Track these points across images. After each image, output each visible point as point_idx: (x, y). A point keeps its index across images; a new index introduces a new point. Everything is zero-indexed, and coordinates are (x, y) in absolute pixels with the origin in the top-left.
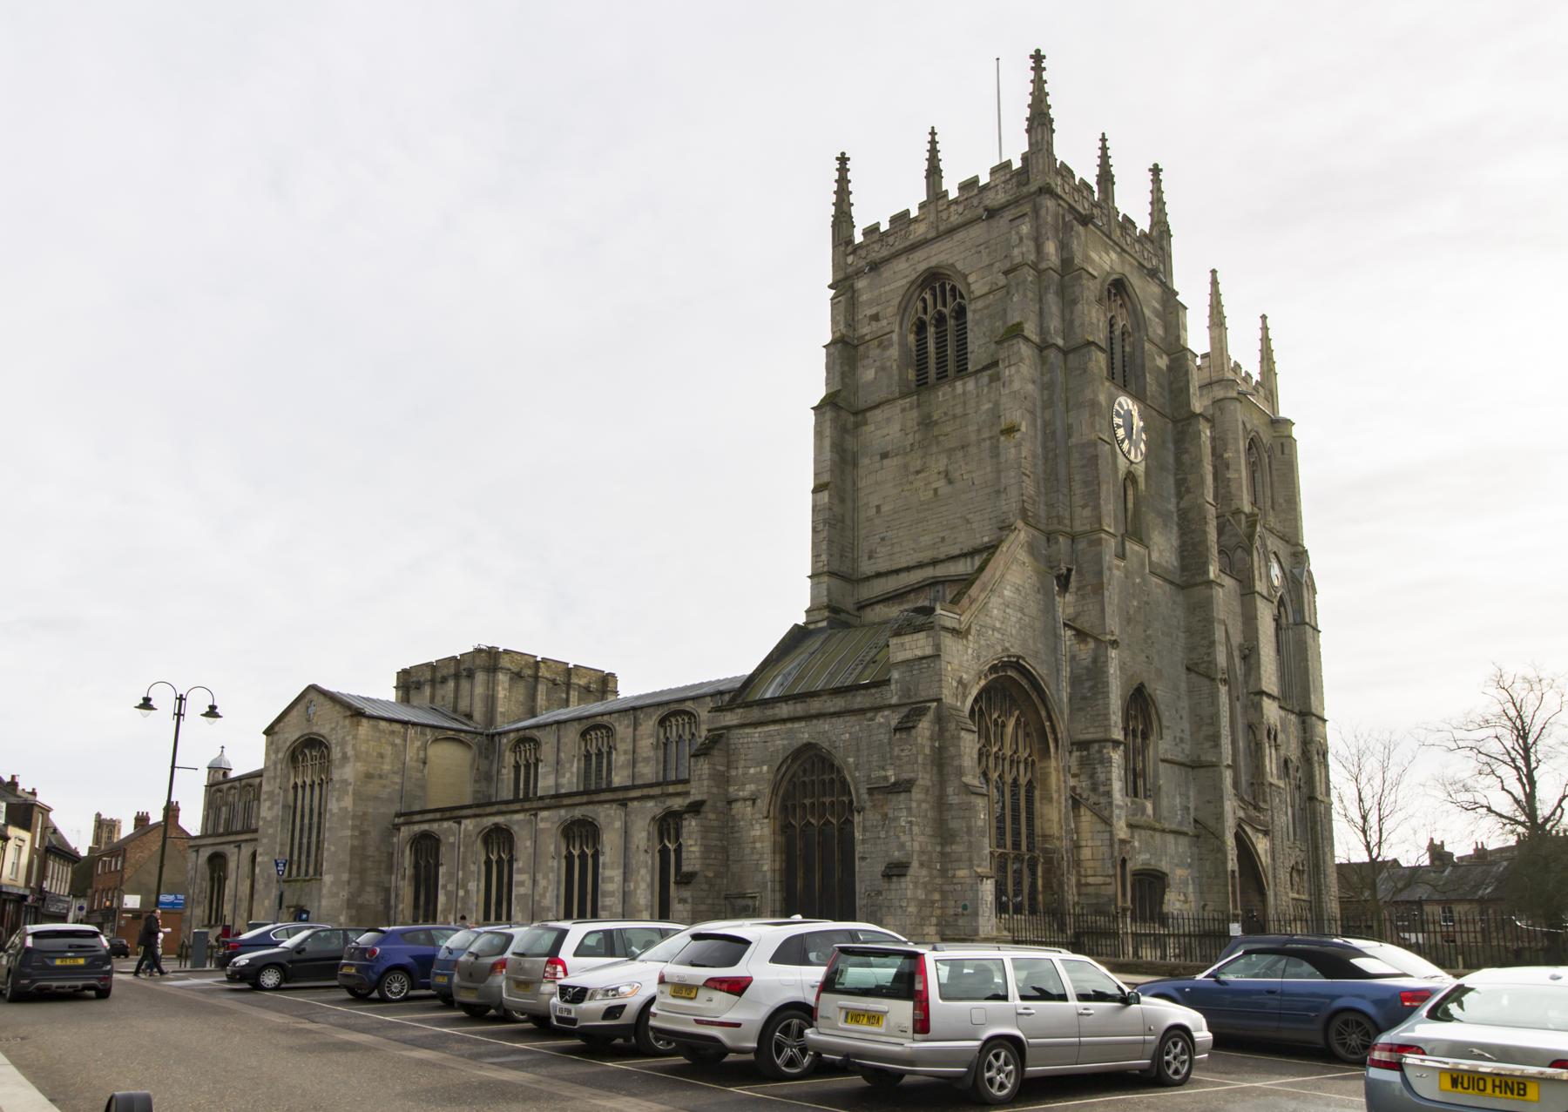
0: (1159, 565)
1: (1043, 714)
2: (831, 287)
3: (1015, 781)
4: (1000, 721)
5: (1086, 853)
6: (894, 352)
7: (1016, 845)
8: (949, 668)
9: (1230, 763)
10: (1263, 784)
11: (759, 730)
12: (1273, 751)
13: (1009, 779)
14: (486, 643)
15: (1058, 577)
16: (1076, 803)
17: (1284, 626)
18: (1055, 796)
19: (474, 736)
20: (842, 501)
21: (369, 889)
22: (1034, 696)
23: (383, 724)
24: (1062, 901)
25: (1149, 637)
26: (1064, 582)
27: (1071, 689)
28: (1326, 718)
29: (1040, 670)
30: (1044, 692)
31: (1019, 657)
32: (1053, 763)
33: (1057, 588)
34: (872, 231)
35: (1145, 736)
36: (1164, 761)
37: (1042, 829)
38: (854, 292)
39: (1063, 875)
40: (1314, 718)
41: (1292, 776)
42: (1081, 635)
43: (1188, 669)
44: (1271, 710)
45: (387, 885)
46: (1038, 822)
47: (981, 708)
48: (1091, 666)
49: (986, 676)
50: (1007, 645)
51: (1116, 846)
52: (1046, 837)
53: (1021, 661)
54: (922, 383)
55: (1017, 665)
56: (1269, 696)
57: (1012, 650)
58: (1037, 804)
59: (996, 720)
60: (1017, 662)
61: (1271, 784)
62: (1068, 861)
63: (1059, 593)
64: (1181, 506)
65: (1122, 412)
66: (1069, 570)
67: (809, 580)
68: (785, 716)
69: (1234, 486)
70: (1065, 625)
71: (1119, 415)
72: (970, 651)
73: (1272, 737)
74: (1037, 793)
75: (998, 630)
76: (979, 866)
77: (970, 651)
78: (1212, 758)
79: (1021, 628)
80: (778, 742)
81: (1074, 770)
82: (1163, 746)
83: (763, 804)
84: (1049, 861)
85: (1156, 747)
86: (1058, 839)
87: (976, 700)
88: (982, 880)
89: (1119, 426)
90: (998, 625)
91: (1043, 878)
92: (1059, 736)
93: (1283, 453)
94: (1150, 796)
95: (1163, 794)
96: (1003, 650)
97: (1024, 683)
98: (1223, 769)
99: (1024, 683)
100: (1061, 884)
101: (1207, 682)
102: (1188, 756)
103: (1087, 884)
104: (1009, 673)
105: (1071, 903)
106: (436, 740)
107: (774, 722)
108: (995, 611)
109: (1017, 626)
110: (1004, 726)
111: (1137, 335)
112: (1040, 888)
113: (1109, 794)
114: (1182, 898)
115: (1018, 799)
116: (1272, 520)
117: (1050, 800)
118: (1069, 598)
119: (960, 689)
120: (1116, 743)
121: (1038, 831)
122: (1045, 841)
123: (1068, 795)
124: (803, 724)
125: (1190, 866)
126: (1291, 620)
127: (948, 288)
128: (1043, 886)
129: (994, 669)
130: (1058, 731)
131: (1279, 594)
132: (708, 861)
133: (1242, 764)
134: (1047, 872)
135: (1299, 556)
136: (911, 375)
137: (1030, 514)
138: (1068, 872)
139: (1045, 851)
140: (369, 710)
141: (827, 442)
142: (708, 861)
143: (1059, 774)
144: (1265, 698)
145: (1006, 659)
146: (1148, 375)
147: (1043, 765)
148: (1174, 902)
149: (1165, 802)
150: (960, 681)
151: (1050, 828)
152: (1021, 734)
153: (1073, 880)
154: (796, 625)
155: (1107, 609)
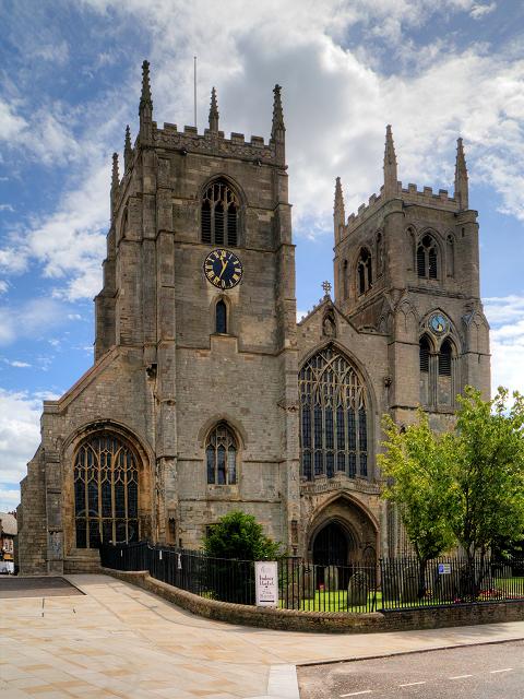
1: (138, 446)
7: (120, 513)
13: (113, 483)
18: (146, 488)
25: (236, 391)
29: (130, 424)
32: (145, 471)
34: (352, 218)
35: (234, 448)
63: (149, 380)
71: (210, 263)
82: (249, 451)
84: (143, 522)
89: (209, 270)
100: (150, 534)
110: (109, 455)
134: (143, 527)
143: (147, 477)
149: (247, 485)
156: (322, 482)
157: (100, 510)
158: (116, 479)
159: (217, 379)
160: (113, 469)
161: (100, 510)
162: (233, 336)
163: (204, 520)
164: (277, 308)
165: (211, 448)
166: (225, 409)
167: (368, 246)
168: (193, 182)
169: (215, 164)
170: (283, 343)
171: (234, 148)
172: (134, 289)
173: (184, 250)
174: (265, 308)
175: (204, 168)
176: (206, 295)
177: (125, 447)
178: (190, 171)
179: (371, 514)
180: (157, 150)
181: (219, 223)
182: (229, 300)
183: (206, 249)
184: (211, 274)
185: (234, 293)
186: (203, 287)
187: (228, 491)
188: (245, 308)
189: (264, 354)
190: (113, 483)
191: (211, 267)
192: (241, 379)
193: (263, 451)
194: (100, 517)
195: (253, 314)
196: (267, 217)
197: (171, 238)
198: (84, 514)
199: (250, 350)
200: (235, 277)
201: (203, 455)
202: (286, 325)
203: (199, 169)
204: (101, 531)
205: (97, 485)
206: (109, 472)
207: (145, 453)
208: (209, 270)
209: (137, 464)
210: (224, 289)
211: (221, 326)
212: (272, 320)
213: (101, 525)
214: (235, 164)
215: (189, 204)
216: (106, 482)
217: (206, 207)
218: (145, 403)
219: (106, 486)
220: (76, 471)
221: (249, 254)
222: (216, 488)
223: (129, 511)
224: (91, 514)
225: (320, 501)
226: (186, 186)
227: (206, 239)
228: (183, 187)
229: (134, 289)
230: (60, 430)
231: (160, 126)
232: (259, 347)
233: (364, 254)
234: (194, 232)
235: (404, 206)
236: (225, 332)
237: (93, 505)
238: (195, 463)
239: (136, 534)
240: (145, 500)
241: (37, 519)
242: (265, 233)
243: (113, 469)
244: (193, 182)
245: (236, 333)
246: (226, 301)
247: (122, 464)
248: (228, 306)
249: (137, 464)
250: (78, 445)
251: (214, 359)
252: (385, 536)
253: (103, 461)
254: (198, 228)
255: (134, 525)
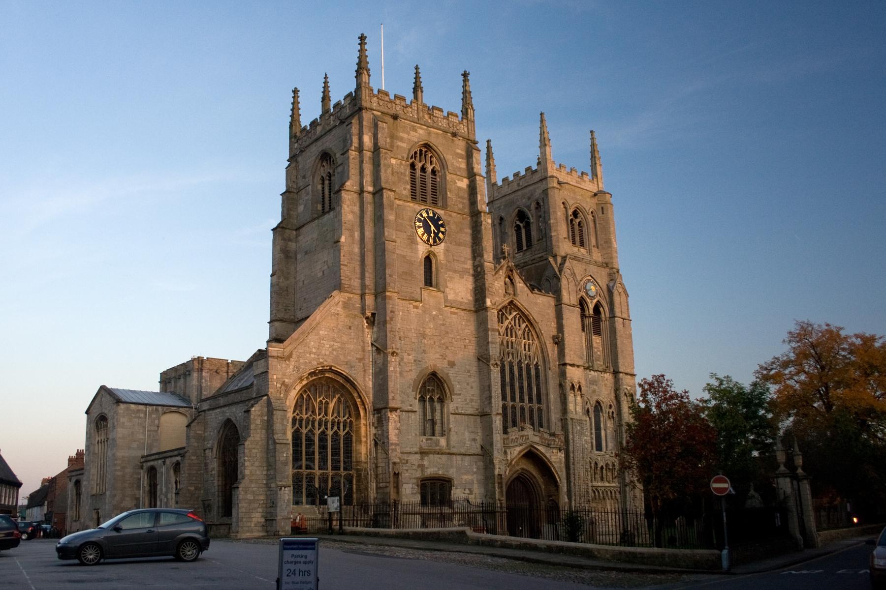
0: (455, 301)
1: (355, 395)
2: (288, 161)
3: (336, 433)
4: (324, 401)
5: (380, 469)
6: (310, 197)
7: (336, 468)
8: (275, 377)
9: (500, 411)
10: (566, 419)
11: (214, 412)
12: (579, 398)
13: (330, 433)
14: (196, 356)
15: (367, 318)
16: (376, 444)
17: (604, 319)
18: (364, 439)
19: (188, 409)
20: (287, 279)
21: (127, 499)
22: (348, 386)
23: (133, 406)
24: (367, 497)
26: (371, 321)
27: (375, 380)
28: (635, 373)
30: (354, 383)
31: (332, 366)
32: (363, 421)
33: (366, 324)
35: (441, 400)
36: (452, 414)
37: (356, 458)
38: (297, 162)
39: (368, 483)
40: (621, 374)
41: (604, 411)
42: (378, 350)
43: (479, 359)
44: (574, 374)
45: (138, 496)
46: (354, 454)
47: (308, 396)
48: (382, 367)
49: (307, 378)
50: (321, 360)
51: (391, 466)
52: (358, 462)
53: (333, 368)
54: (324, 213)
55: (331, 370)
56: (573, 365)
57: (325, 363)
58: (354, 445)
59: (321, 401)
60: (331, 369)
61: (572, 419)
62: (371, 475)
63: (367, 327)
64: (475, 264)
65: (423, 219)
66: (373, 314)
67: (268, 324)
68: (222, 405)
69: (554, 239)
70: (372, 344)
71: (420, 220)
72: (291, 367)
73: (576, 390)
74: (354, 438)
75: (315, 354)
76: (281, 481)
77: (291, 367)
78: (487, 410)
79: (334, 350)
80: (220, 418)
81: (376, 425)
83: (215, 449)
84: (359, 476)
85: (448, 406)
86: (364, 463)
87: (305, 391)
88: (281, 489)
90: (314, 350)
91: (356, 485)
92: (366, 406)
93: (603, 213)
94: (445, 435)
95: (452, 433)
96: (318, 364)
97: (339, 379)
98: (494, 417)
99: (339, 379)
100: (366, 488)
101: (486, 366)
102: (477, 409)
103: (381, 488)
104: (327, 375)
105: (372, 498)
106: (165, 413)
107: (219, 407)
108: (312, 343)
109: (330, 349)
110: (327, 403)
111: (443, 171)
112: (355, 490)
113: (387, 437)
114: (467, 491)
115: (339, 443)
116: (597, 256)
117: (360, 442)
118: (375, 329)
119: (283, 387)
120: (395, 409)
121: (354, 459)
122: (357, 465)
123: (372, 438)
124: (227, 408)
125: (475, 473)
126: (608, 315)
127: (332, 160)
128: (356, 490)
129: (311, 374)
130: (365, 403)
131: (595, 301)
132: (190, 482)
133: (553, 408)
134: (358, 481)
135: (613, 275)
136: (320, 207)
137: (346, 286)
138: (371, 480)
139: (357, 470)
140: (124, 399)
141: (278, 248)
142: (190, 482)
143: (365, 428)
144: (568, 367)
145: (321, 368)
146: (449, 193)
147: (358, 423)
148: (457, 493)
149: (454, 438)
150: (283, 383)
151: (361, 457)
152: (341, 406)
153: (374, 485)
154: (259, 350)
155: (388, 335)
156: (514, 433)
157: (317, 461)
158: (332, 429)
159: (427, 331)
160: (330, 418)
161: (317, 461)
162: (439, 290)
163: (419, 474)
164: (475, 267)
165: (422, 400)
166: (434, 360)
167: (526, 210)
168: (404, 145)
169: (421, 131)
170: (484, 302)
171: (435, 118)
172: (352, 236)
173: (398, 205)
174: (466, 266)
175: (412, 133)
176: (417, 251)
177: (342, 395)
178: (402, 135)
179: (554, 468)
180: (375, 112)
181: (424, 183)
182: (435, 255)
183: (418, 207)
184: (421, 231)
185: (440, 249)
186: (412, 241)
187: (437, 443)
188: (449, 265)
189: (465, 310)
190: (330, 433)
191: (421, 224)
192: (447, 333)
193: (467, 404)
194: (317, 472)
195: (455, 271)
196: (463, 184)
197: (391, 194)
198: (300, 467)
199: (454, 305)
200: (440, 235)
201: (417, 406)
202: (487, 285)
203: (408, 133)
204: (317, 485)
205: (314, 434)
206: (326, 422)
207: (363, 404)
208: (419, 227)
209: (353, 413)
210: (431, 246)
211: (429, 282)
212: (471, 279)
213: (317, 480)
214: (438, 134)
215: (401, 164)
216: (323, 433)
217: (413, 166)
218: (364, 351)
219: (323, 438)
220: (294, 420)
221: (450, 216)
222: (427, 440)
223: (345, 463)
224: (308, 467)
225: (516, 452)
226: (398, 147)
227: (414, 197)
228: (395, 148)
229: (352, 236)
230: (284, 374)
231: (376, 92)
232: (461, 303)
233: (522, 216)
234: (405, 189)
235: (559, 183)
236: (431, 286)
237: (310, 456)
238: (410, 414)
239: (351, 489)
240: (363, 450)
241: (258, 472)
242: (463, 198)
243: (330, 418)
244: (404, 145)
245: (442, 289)
246: (432, 257)
247: (338, 413)
248: (434, 262)
249: (353, 413)
250: (299, 392)
251: (424, 312)
252: (565, 489)
253: (320, 409)
254: (409, 187)
255: (349, 479)
